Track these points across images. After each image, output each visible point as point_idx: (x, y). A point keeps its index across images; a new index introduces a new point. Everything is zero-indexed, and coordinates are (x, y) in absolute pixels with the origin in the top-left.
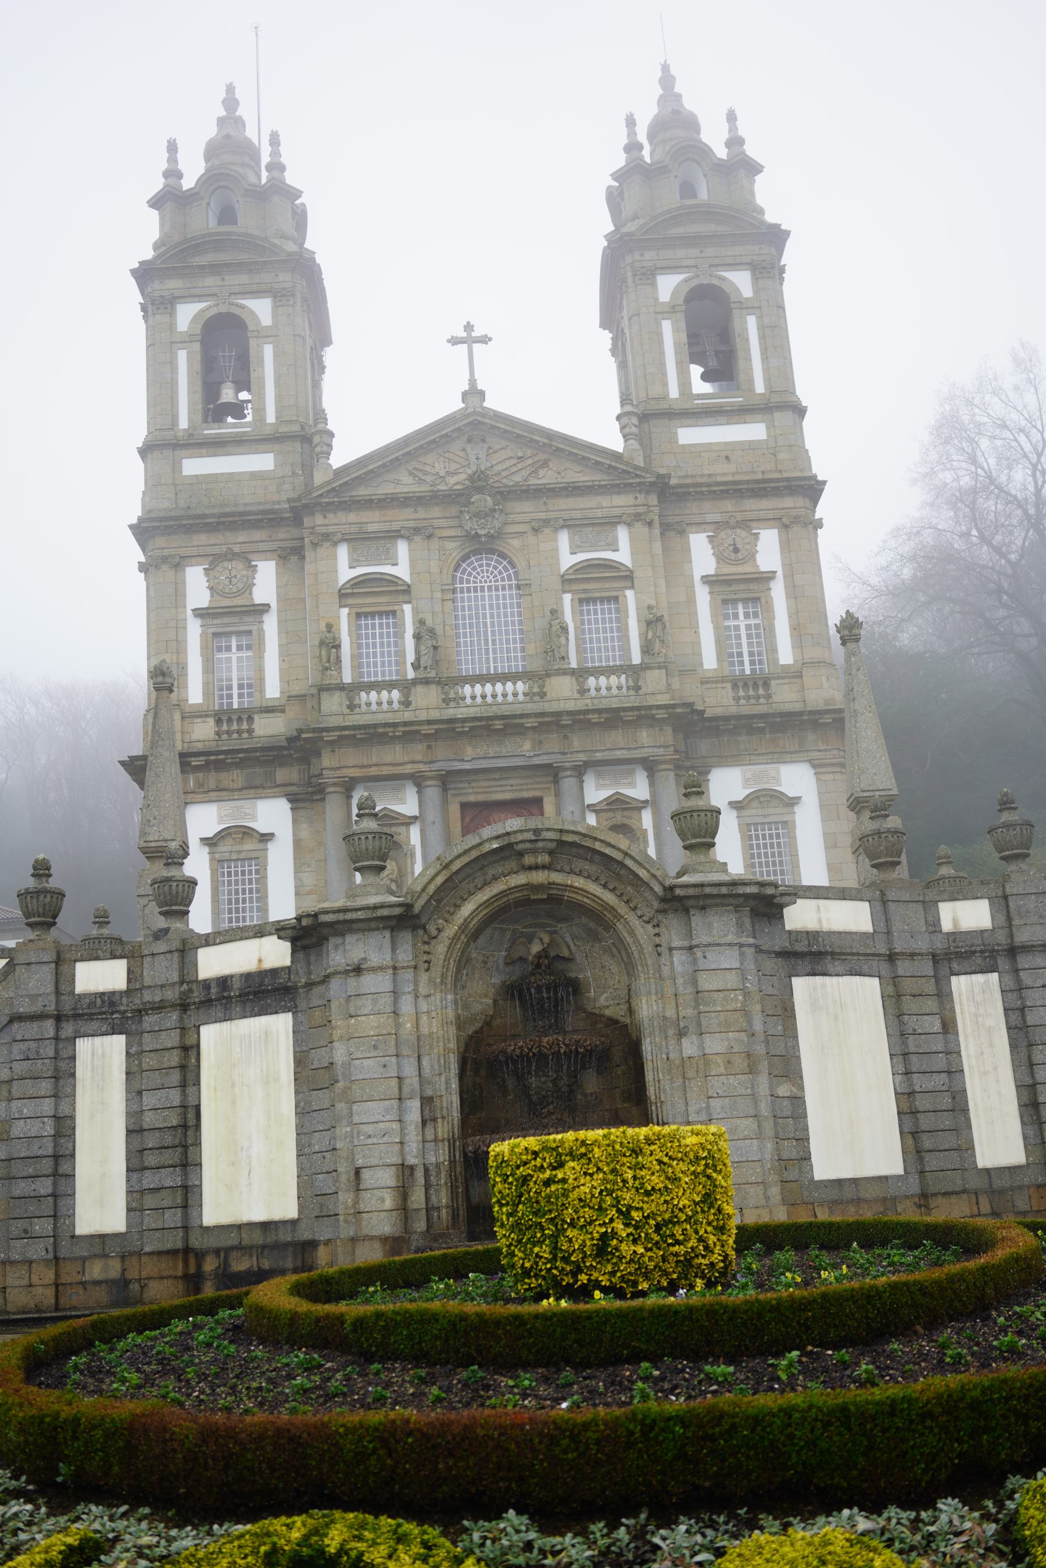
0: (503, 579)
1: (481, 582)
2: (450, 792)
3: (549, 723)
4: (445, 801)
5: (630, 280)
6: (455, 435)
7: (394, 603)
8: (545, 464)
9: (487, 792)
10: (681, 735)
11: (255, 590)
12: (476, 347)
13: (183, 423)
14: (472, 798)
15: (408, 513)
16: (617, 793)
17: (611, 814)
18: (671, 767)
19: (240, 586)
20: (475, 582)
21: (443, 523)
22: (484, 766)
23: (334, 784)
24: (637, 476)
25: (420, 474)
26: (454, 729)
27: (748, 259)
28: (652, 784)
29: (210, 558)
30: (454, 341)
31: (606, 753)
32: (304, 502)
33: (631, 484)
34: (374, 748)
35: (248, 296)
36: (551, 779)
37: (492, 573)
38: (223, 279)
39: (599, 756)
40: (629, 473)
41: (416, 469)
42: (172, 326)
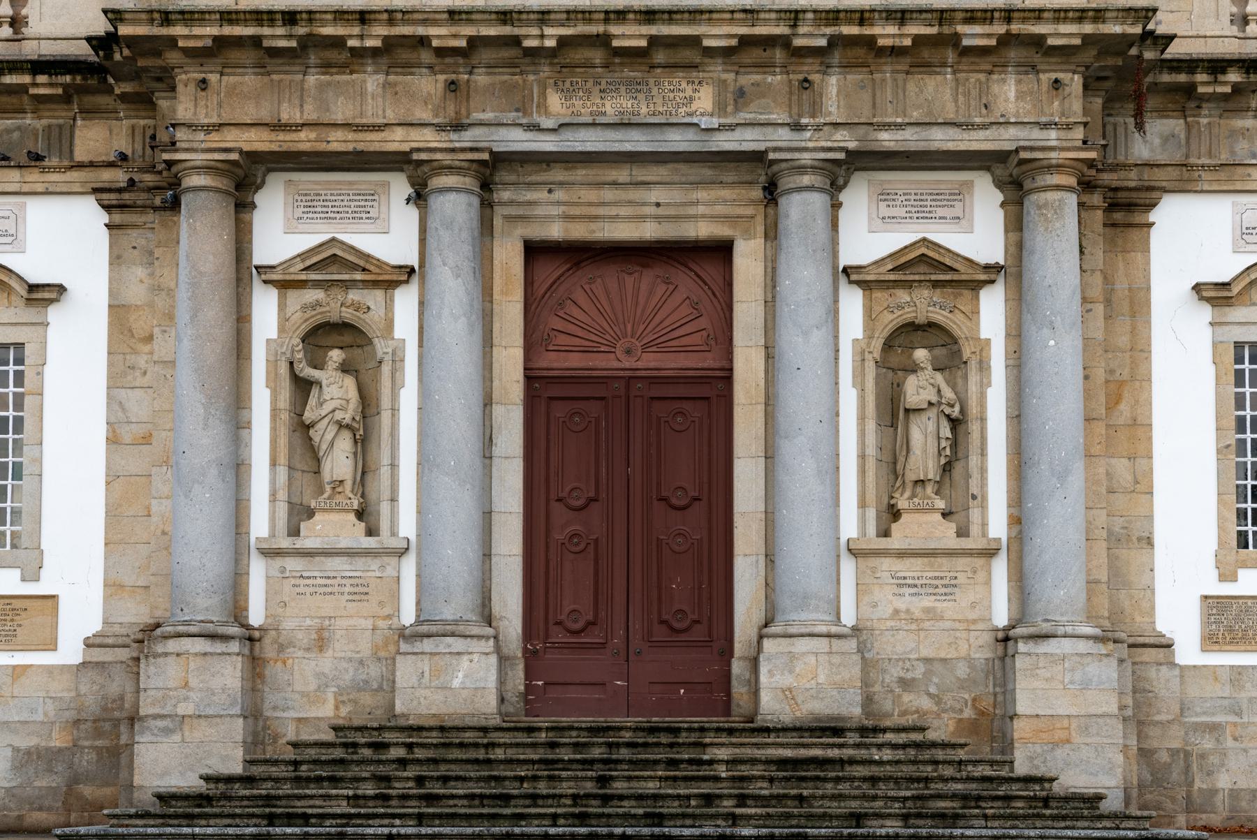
2: (499, 211)
3: (768, 42)
4: (486, 228)
9: (595, 218)
10: (1098, 102)
14: (556, 232)
16: (924, 239)
17: (903, 296)
18: (1072, 181)
22: (589, 147)
23: (199, 169)
26: (516, 41)
28: (1016, 224)
31: (908, 134)
34: (312, 79)
36: (757, 193)
39: (887, 140)
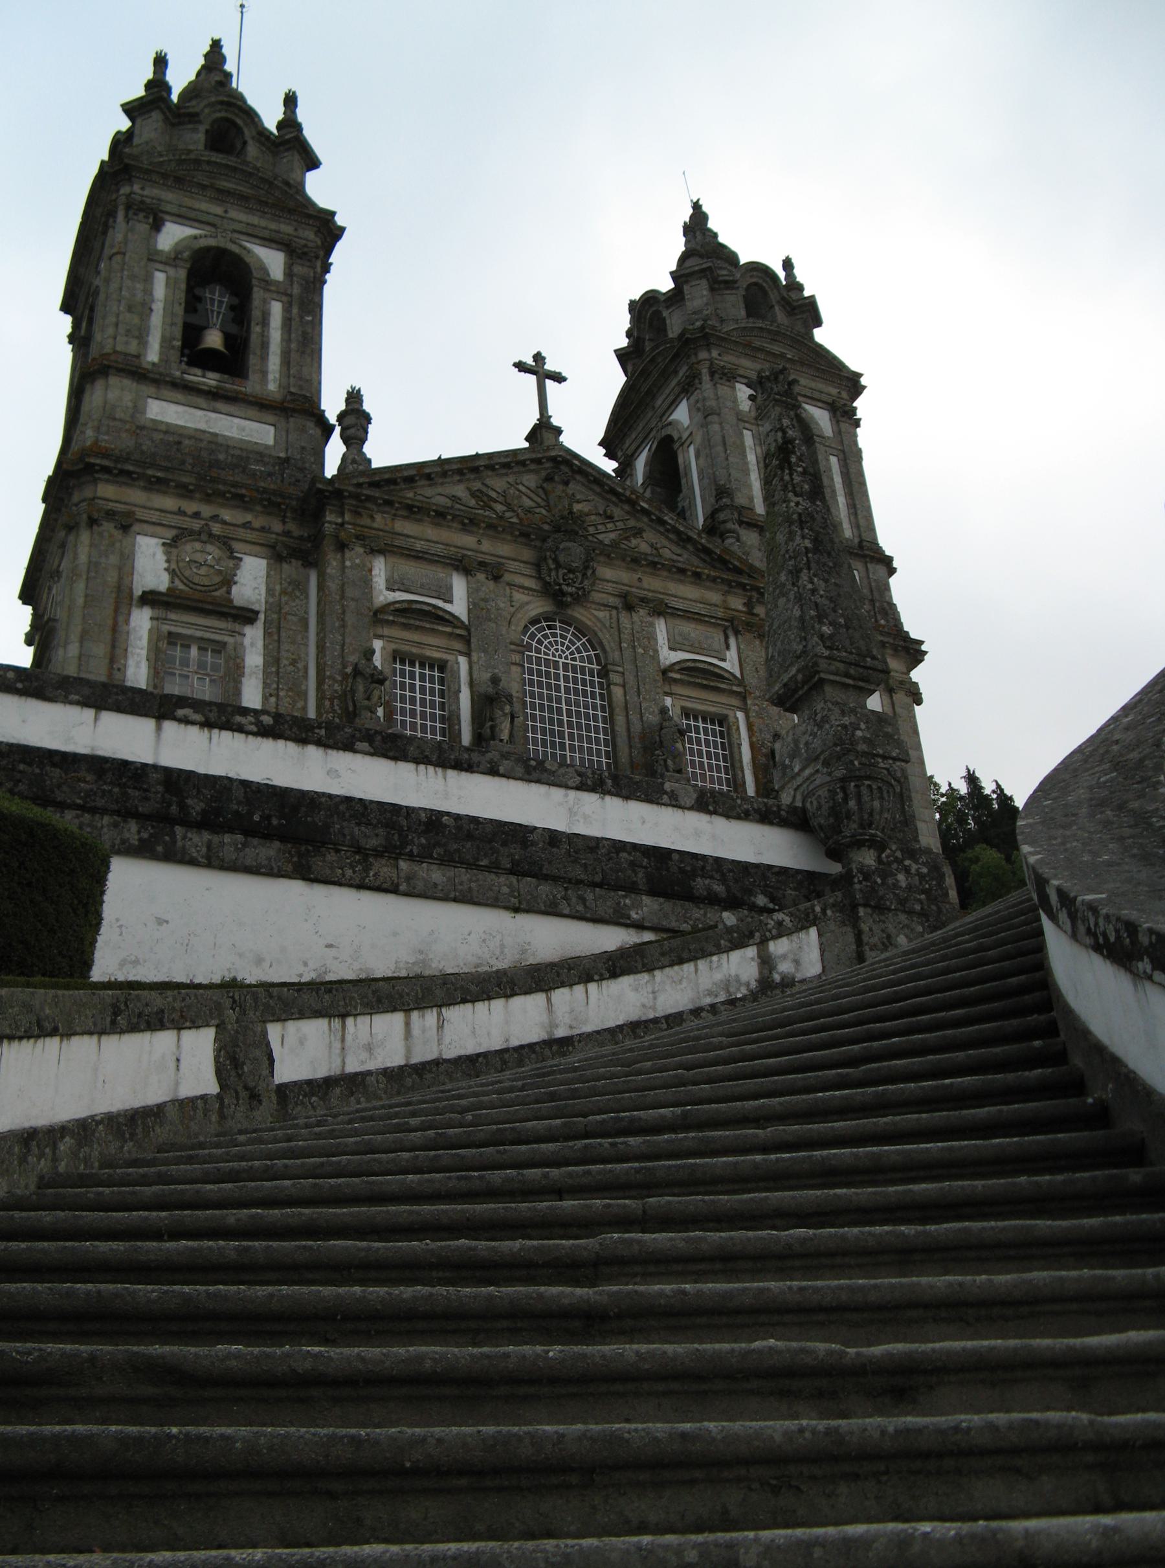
0: (582, 659)
1: (554, 656)
5: (706, 377)
6: (533, 467)
7: (450, 650)
8: (638, 533)
11: (235, 589)
12: (549, 384)
13: (153, 355)
15: (468, 540)
19: (217, 579)
20: (546, 654)
21: (513, 565)
24: (751, 577)
25: (485, 499)
27: (824, 397)
30: (521, 366)
32: (336, 485)
35: (258, 241)
37: (568, 648)
38: (226, 212)
40: (739, 571)
41: (482, 492)
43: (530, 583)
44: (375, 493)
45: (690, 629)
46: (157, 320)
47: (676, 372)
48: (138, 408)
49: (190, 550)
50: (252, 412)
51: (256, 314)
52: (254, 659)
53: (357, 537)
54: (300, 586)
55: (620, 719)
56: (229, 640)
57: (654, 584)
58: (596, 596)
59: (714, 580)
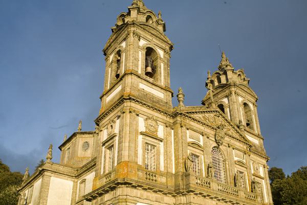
29: (146, 117)
33: (247, 144)
42: (138, 43)
43: (214, 140)
44: (187, 114)
45: (238, 152)
46: (140, 63)
47: (225, 91)
48: (138, 85)
49: (149, 121)
50: (159, 89)
51: (159, 65)
52: (162, 151)
53: (185, 125)
54: (170, 134)
55: (228, 172)
56: (157, 145)
57: (233, 142)
58: (224, 144)
59: (242, 142)
